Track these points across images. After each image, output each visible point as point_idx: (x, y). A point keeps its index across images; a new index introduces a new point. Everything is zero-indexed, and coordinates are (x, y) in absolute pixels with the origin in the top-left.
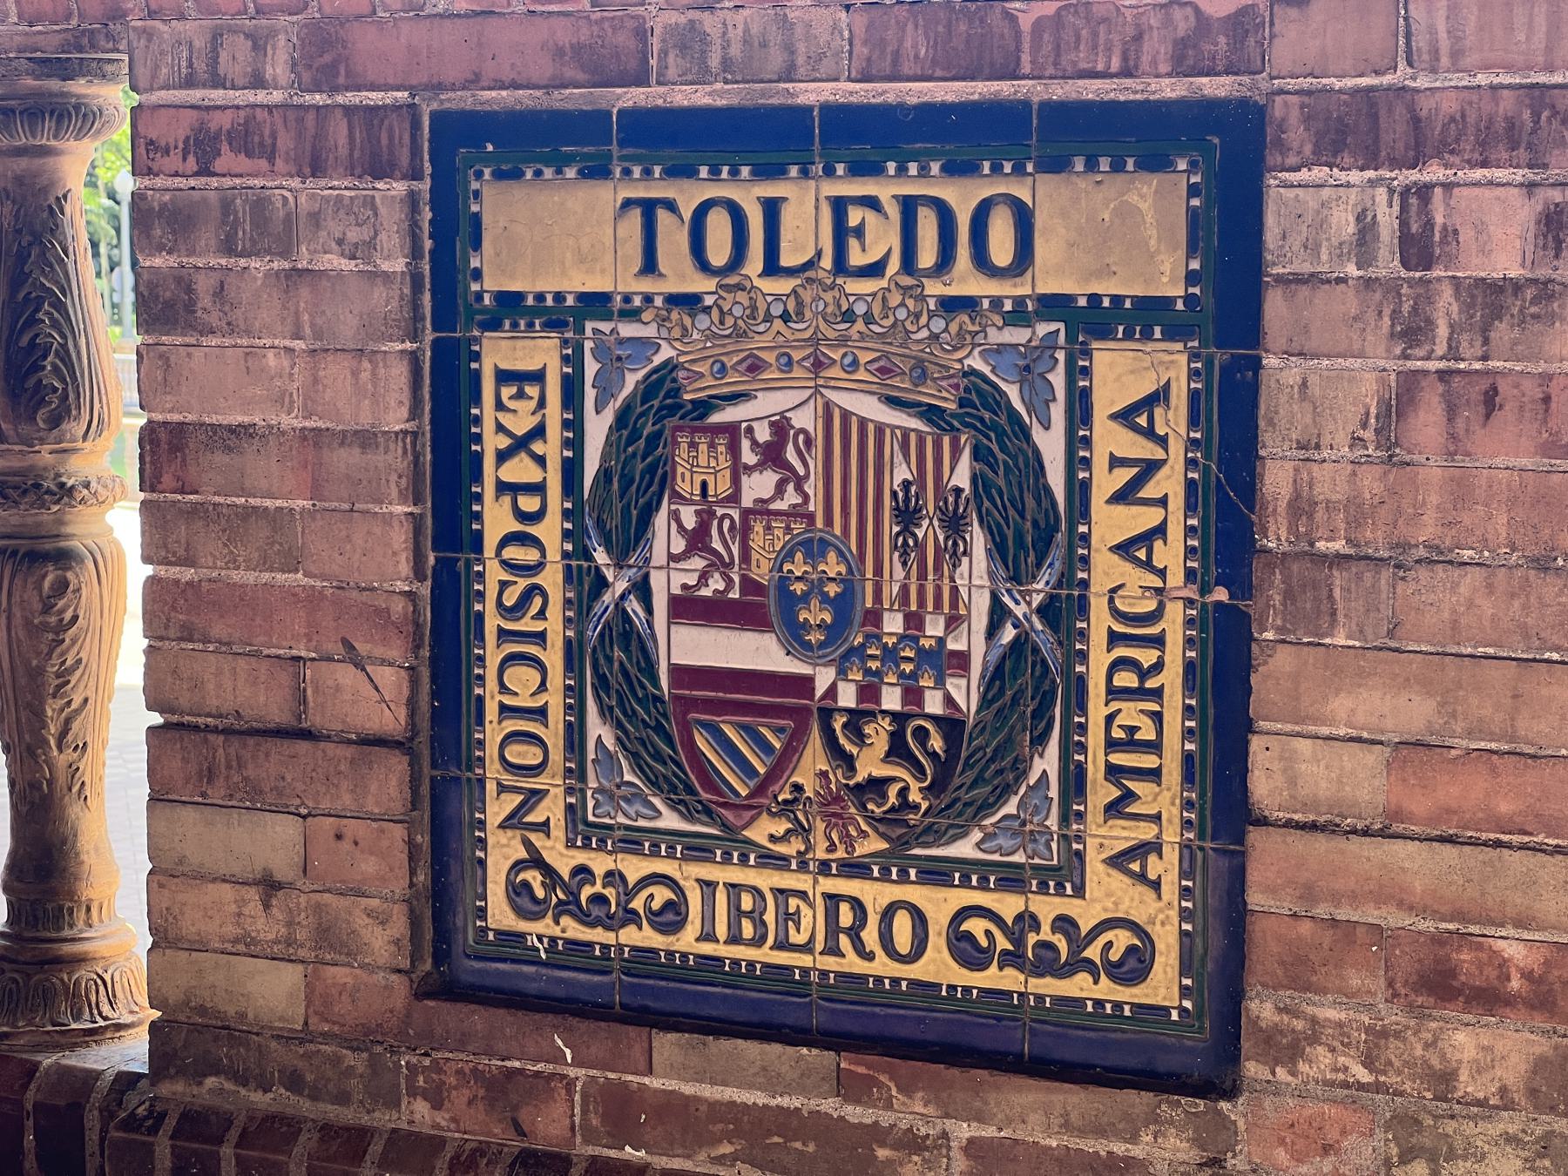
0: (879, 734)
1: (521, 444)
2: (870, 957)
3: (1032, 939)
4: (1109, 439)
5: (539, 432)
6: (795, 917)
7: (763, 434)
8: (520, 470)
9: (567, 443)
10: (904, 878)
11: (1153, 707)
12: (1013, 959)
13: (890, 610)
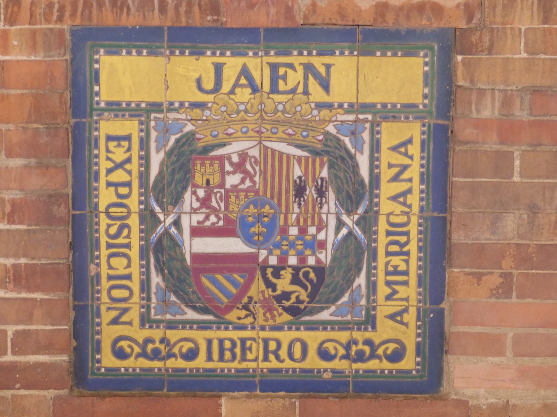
0: (287, 274)
1: (120, 166)
2: (282, 361)
3: (354, 348)
4: (386, 156)
5: (129, 160)
6: (250, 349)
7: (235, 159)
8: (119, 176)
9: (141, 165)
10: (298, 329)
11: (406, 257)
12: (346, 357)
13: (292, 225)
